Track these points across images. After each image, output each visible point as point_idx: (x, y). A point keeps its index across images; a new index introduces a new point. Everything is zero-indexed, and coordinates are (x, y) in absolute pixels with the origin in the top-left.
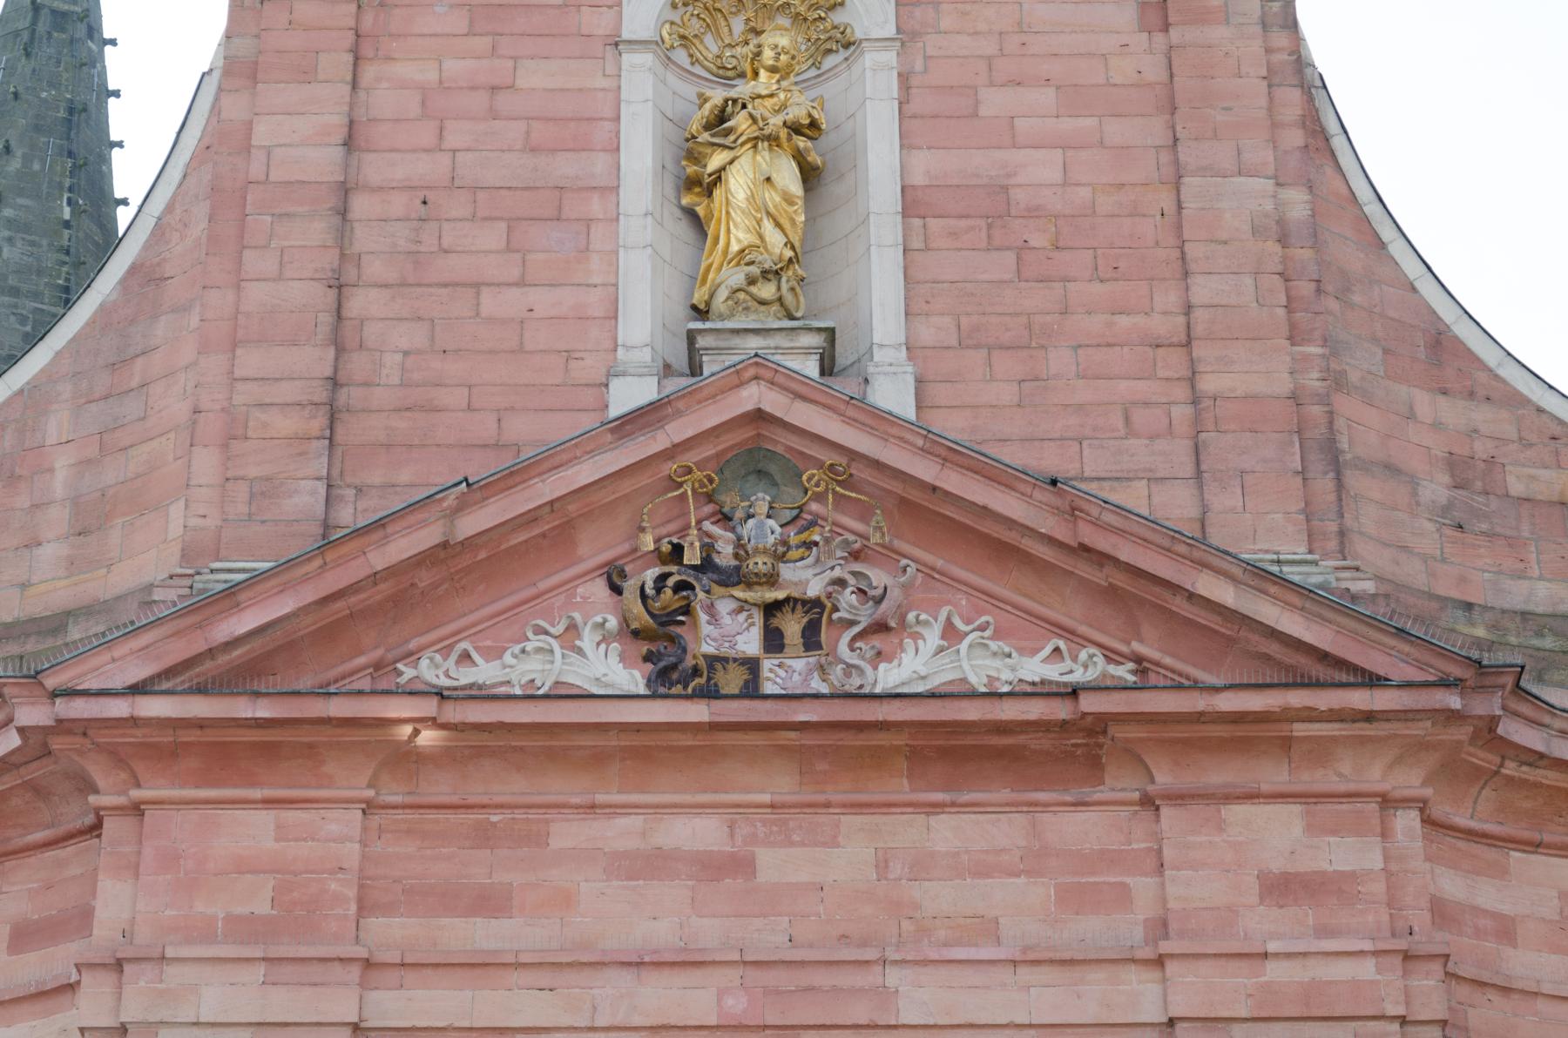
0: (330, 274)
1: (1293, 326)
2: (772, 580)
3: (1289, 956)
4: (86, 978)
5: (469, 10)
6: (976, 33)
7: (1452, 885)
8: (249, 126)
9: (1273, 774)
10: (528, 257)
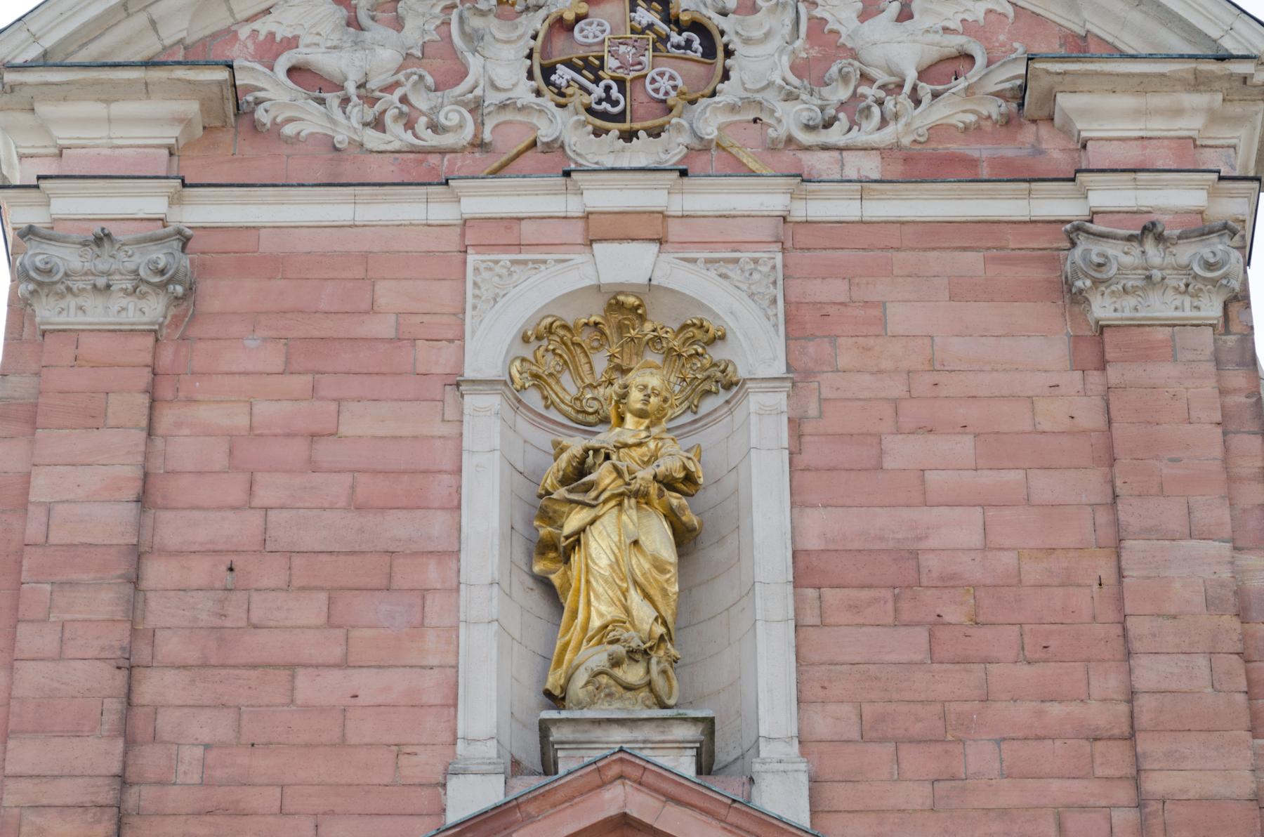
0: (119, 653)
5: (285, 344)
6: (880, 372)
8: (27, 478)
10: (355, 633)
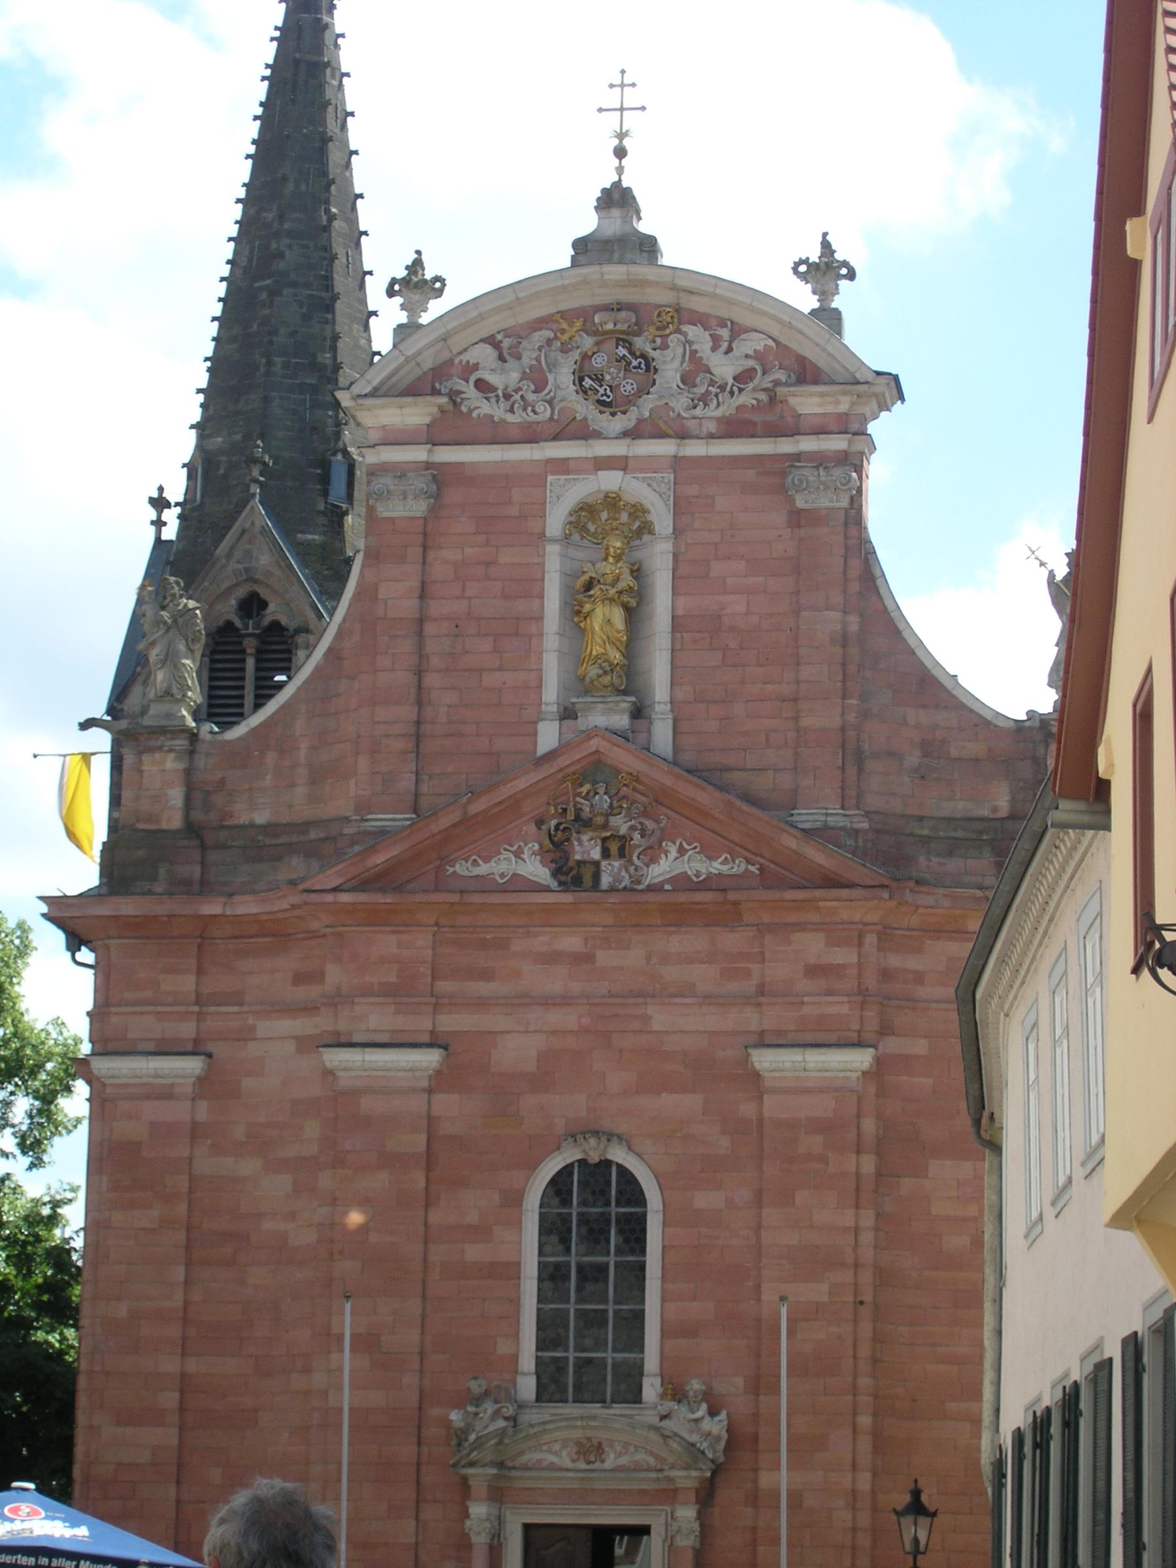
1: (844, 689)
2: (605, 826)
7: (894, 961)
9: (814, 917)
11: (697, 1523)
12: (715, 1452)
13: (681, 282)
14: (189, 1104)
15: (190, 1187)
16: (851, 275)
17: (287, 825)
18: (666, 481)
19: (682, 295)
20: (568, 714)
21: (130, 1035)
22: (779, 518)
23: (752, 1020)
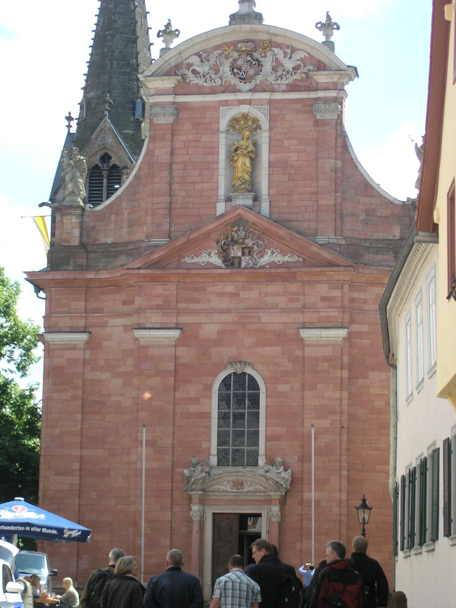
2: (243, 243)
3: (324, 312)
4: (134, 315)
7: (355, 295)
8: (154, 151)
11: (280, 512)
12: (286, 485)
13: (272, 31)
14: (82, 351)
15: (83, 384)
16: (338, 28)
17: (120, 243)
18: (266, 109)
19: (272, 36)
20: (228, 199)
21: (59, 325)
22: (310, 123)
23: (300, 318)
